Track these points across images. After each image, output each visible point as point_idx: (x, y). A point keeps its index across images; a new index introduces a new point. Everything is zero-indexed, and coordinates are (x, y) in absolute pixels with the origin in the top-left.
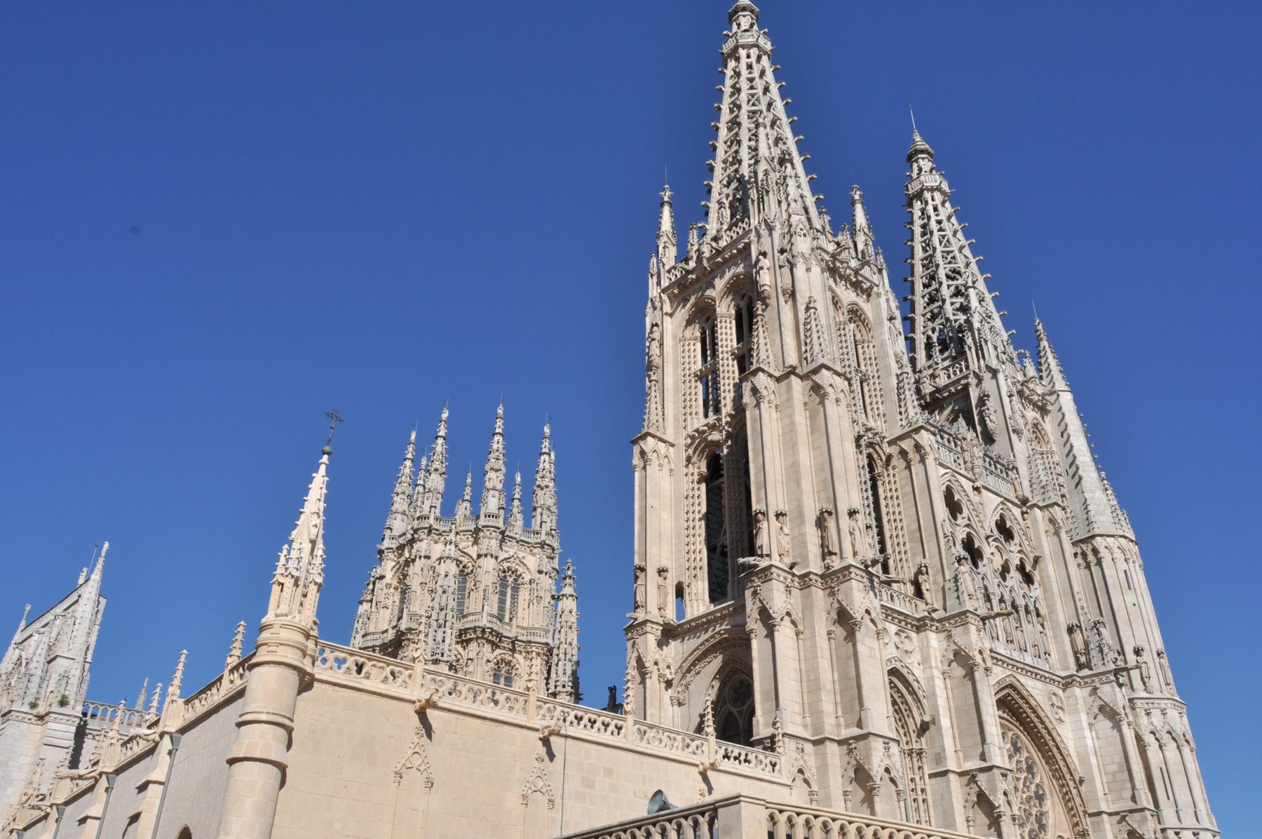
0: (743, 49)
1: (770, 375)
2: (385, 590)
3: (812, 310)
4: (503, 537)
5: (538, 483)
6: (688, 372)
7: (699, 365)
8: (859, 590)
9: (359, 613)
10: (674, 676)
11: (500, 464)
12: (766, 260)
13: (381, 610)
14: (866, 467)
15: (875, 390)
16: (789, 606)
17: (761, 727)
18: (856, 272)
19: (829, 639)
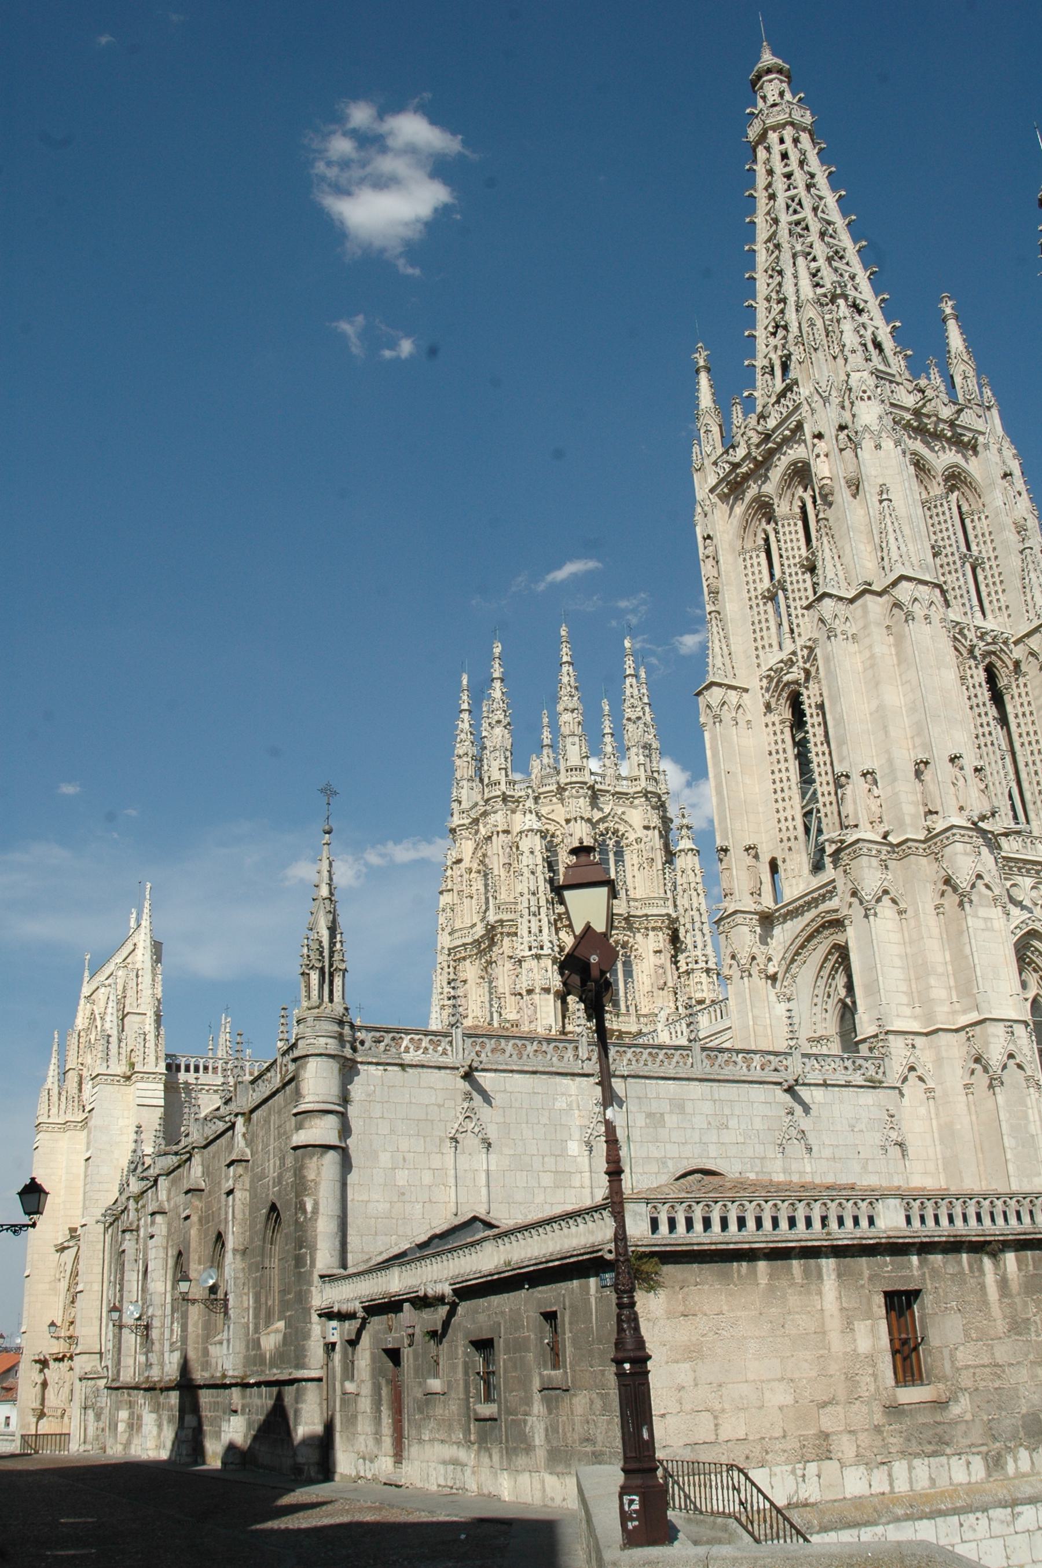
0: (775, 131)
1: (841, 599)
2: (466, 876)
3: (885, 503)
4: (594, 792)
5: (626, 716)
6: (753, 594)
7: (766, 583)
8: (966, 854)
9: (441, 906)
10: (776, 970)
11: (574, 703)
12: (823, 444)
13: (465, 900)
14: (984, 684)
15: (993, 576)
16: (885, 883)
17: (865, 1025)
18: (952, 424)
19: (938, 914)
